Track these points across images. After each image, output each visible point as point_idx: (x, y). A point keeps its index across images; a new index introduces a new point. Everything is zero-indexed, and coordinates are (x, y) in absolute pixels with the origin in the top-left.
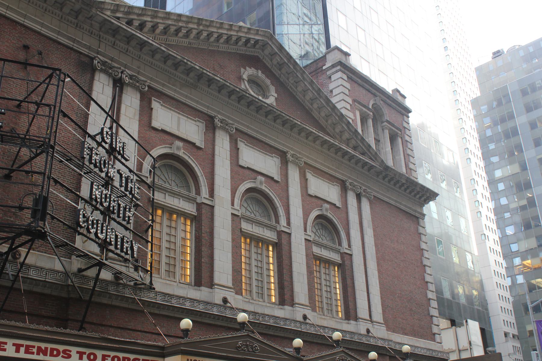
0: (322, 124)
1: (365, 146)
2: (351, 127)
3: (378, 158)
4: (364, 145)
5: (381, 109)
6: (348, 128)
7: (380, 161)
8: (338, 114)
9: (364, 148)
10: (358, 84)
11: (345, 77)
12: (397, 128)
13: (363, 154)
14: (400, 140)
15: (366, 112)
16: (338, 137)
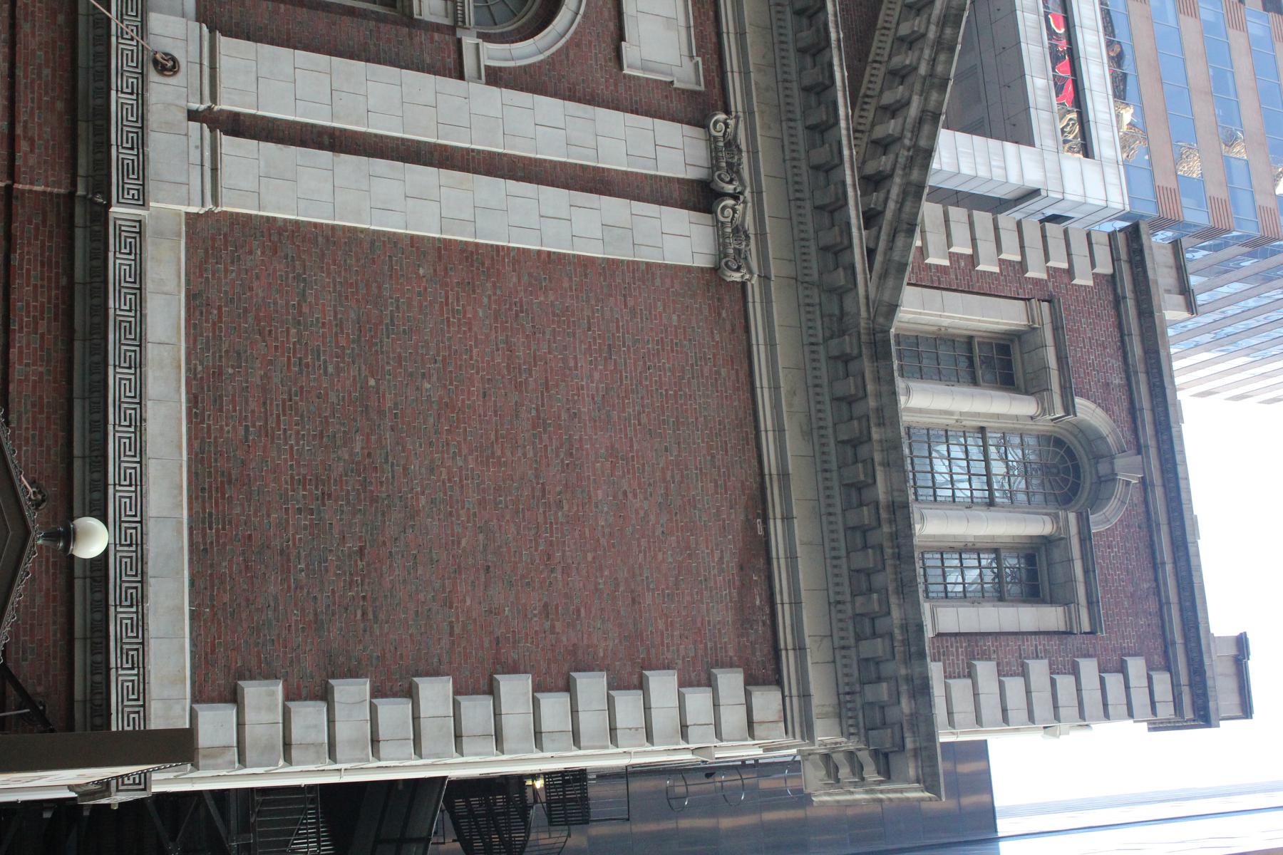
0: (875, 44)
1: (900, 210)
2: (926, 128)
3: (890, 282)
4: (901, 204)
5: (1109, 499)
6: (920, 121)
7: (886, 296)
8: (940, 69)
9: (892, 205)
10: (1122, 341)
11: (1105, 268)
12: (1091, 603)
13: (871, 218)
14: (1049, 617)
15: (1046, 368)
16: (870, 115)
